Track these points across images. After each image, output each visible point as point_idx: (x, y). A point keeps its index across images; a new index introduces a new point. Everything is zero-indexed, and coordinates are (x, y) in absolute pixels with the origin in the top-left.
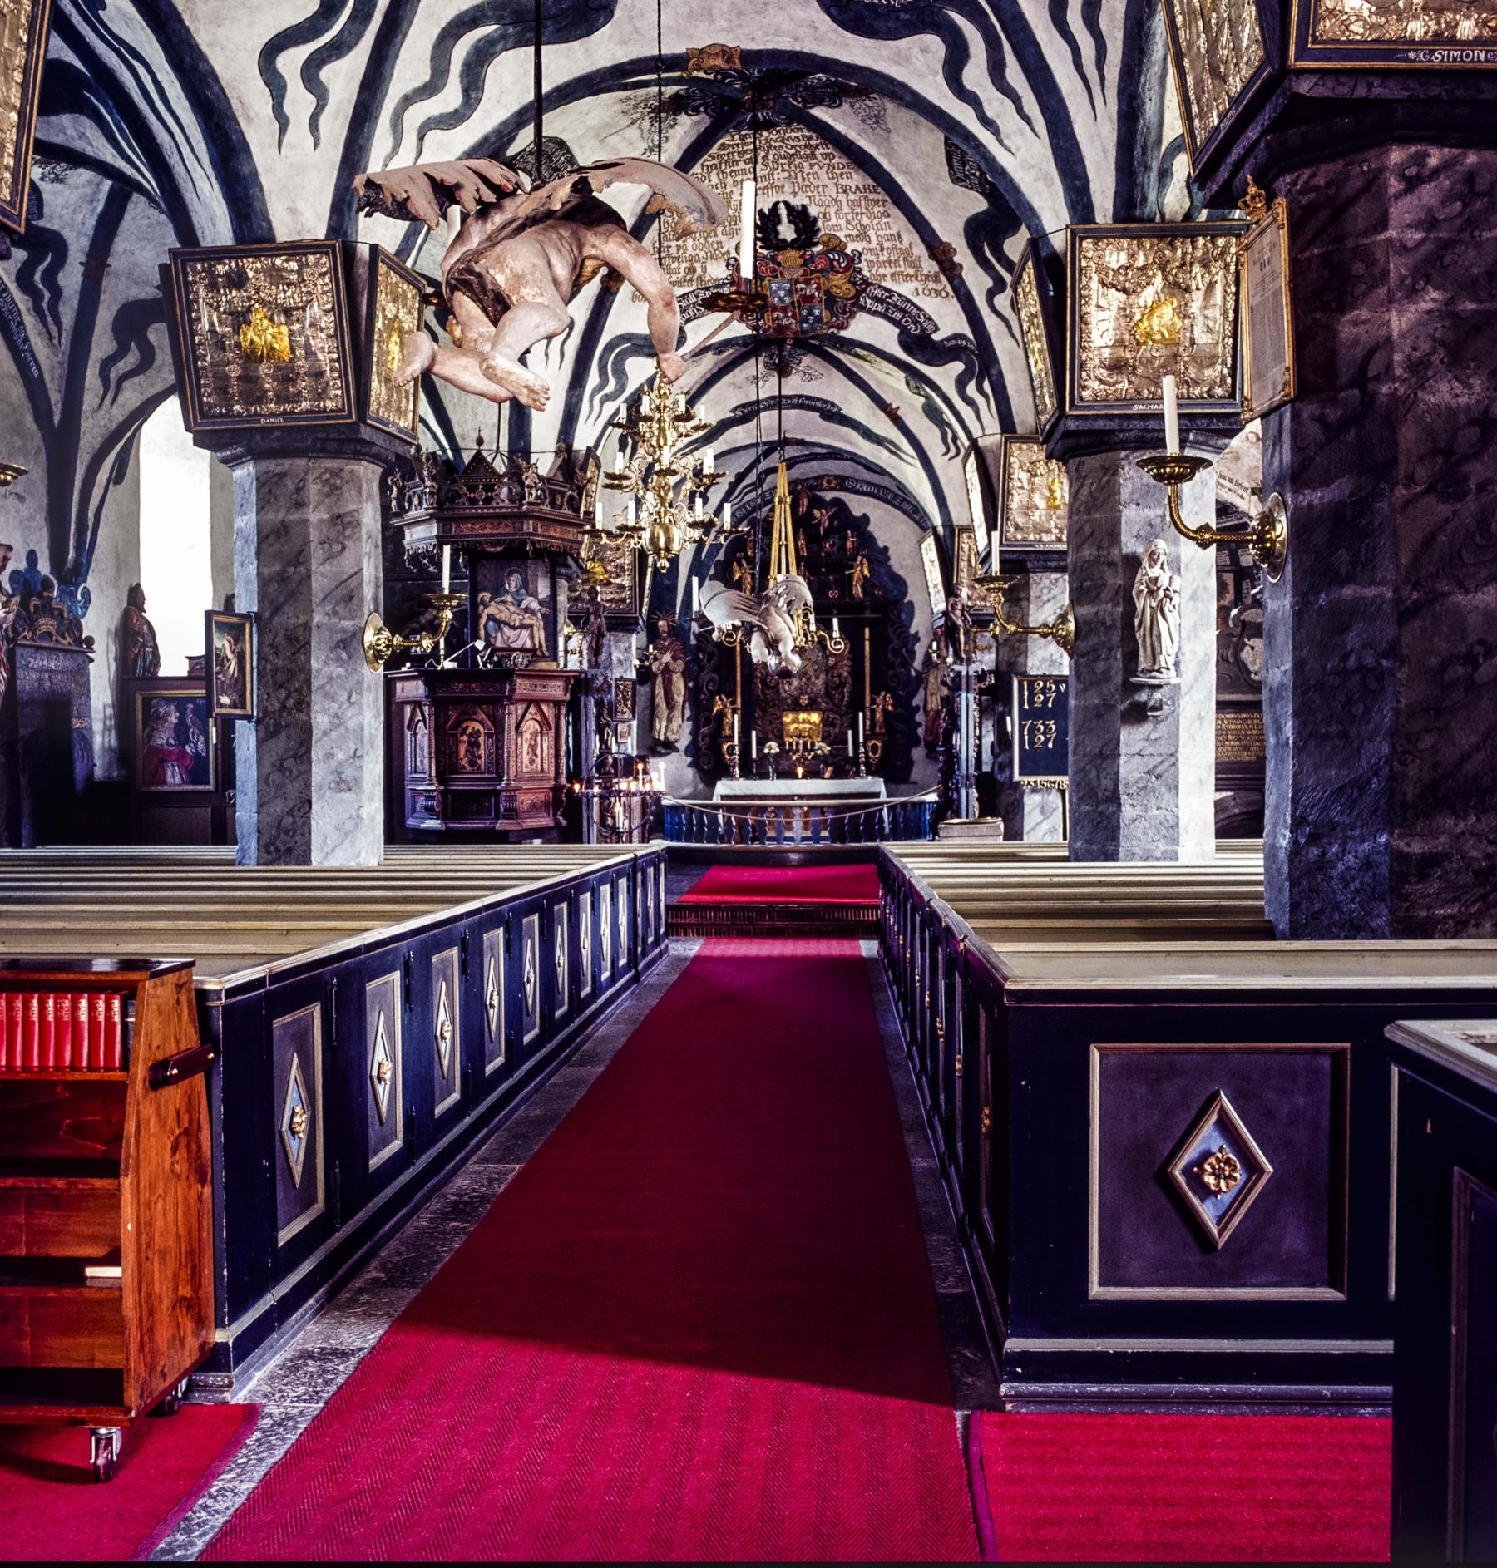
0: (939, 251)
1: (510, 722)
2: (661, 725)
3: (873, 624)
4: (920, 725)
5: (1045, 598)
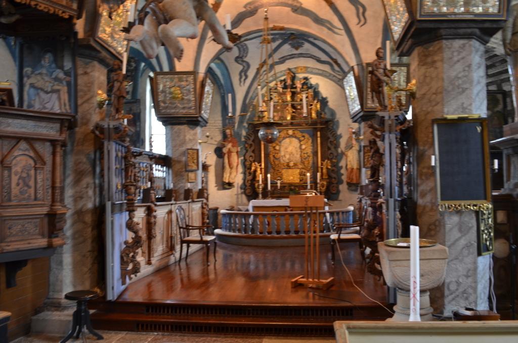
2: (233, 176)
4: (342, 175)
5: (456, 59)
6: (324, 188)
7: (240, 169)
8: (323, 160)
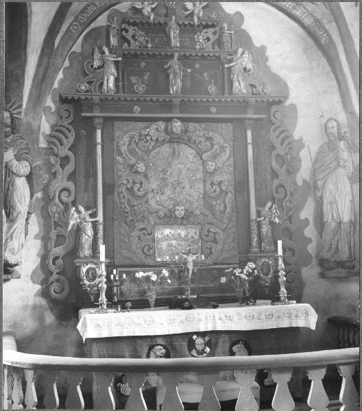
6: (270, 276)
7: (35, 227)
8: (261, 204)
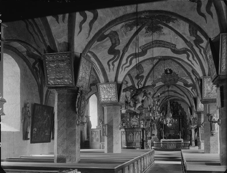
0: (188, 73)
1: (135, 134)
2: (153, 132)
3: (182, 118)
7: (157, 130)
8: (182, 128)
